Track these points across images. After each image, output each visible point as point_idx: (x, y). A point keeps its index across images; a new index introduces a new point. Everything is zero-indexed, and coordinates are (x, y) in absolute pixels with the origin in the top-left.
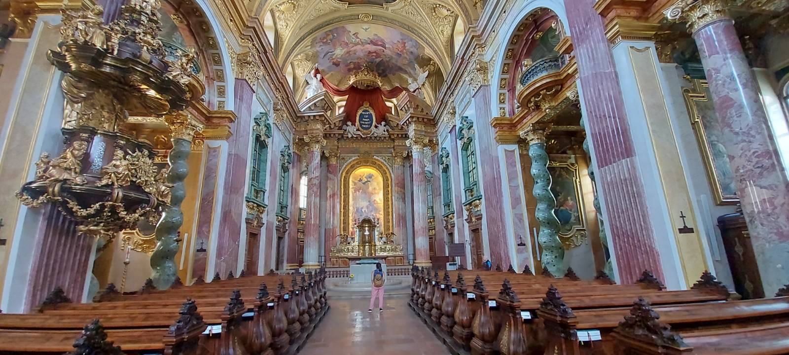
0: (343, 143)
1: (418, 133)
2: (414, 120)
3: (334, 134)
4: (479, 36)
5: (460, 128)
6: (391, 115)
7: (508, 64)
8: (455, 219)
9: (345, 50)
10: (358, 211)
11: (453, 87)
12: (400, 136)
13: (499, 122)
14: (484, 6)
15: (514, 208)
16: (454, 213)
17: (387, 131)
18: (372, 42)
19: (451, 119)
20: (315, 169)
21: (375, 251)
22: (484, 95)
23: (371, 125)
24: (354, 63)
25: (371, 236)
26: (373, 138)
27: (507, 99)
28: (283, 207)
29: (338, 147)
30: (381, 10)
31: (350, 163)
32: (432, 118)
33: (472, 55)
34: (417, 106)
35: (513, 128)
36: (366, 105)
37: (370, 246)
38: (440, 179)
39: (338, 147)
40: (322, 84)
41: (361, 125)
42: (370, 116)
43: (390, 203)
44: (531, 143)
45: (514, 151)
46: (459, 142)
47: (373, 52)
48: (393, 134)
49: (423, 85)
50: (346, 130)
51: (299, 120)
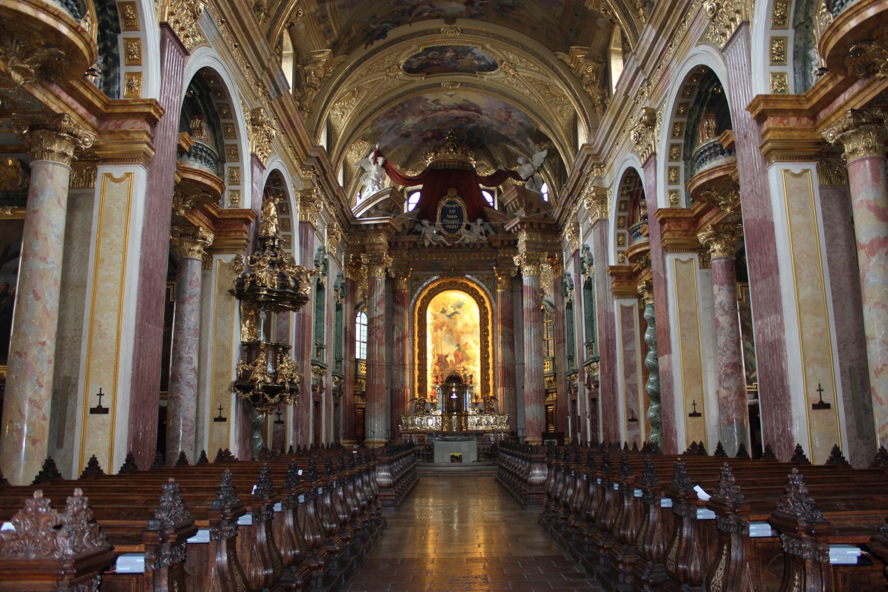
2: (525, 226)
3: (403, 243)
4: (596, 155)
6: (492, 210)
7: (626, 202)
8: (577, 381)
9: (420, 118)
10: (441, 360)
11: (575, 195)
12: (506, 243)
14: (604, 112)
17: (487, 233)
18: (460, 107)
20: (378, 304)
21: (466, 425)
23: (460, 226)
24: (433, 131)
25: (460, 401)
27: (627, 240)
28: (338, 361)
29: (409, 262)
30: (475, 78)
31: (428, 286)
33: (590, 172)
35: (633, 278)
36: (453, 192)
37: (459, 416)
40: (384, 171)
41: (444, 226)
42: (459, 211)
43: (490, 349)
45: (631, 308)
46: (582, 276)
47: (462, 118)
49: (542, 165)
51: (353, 229)
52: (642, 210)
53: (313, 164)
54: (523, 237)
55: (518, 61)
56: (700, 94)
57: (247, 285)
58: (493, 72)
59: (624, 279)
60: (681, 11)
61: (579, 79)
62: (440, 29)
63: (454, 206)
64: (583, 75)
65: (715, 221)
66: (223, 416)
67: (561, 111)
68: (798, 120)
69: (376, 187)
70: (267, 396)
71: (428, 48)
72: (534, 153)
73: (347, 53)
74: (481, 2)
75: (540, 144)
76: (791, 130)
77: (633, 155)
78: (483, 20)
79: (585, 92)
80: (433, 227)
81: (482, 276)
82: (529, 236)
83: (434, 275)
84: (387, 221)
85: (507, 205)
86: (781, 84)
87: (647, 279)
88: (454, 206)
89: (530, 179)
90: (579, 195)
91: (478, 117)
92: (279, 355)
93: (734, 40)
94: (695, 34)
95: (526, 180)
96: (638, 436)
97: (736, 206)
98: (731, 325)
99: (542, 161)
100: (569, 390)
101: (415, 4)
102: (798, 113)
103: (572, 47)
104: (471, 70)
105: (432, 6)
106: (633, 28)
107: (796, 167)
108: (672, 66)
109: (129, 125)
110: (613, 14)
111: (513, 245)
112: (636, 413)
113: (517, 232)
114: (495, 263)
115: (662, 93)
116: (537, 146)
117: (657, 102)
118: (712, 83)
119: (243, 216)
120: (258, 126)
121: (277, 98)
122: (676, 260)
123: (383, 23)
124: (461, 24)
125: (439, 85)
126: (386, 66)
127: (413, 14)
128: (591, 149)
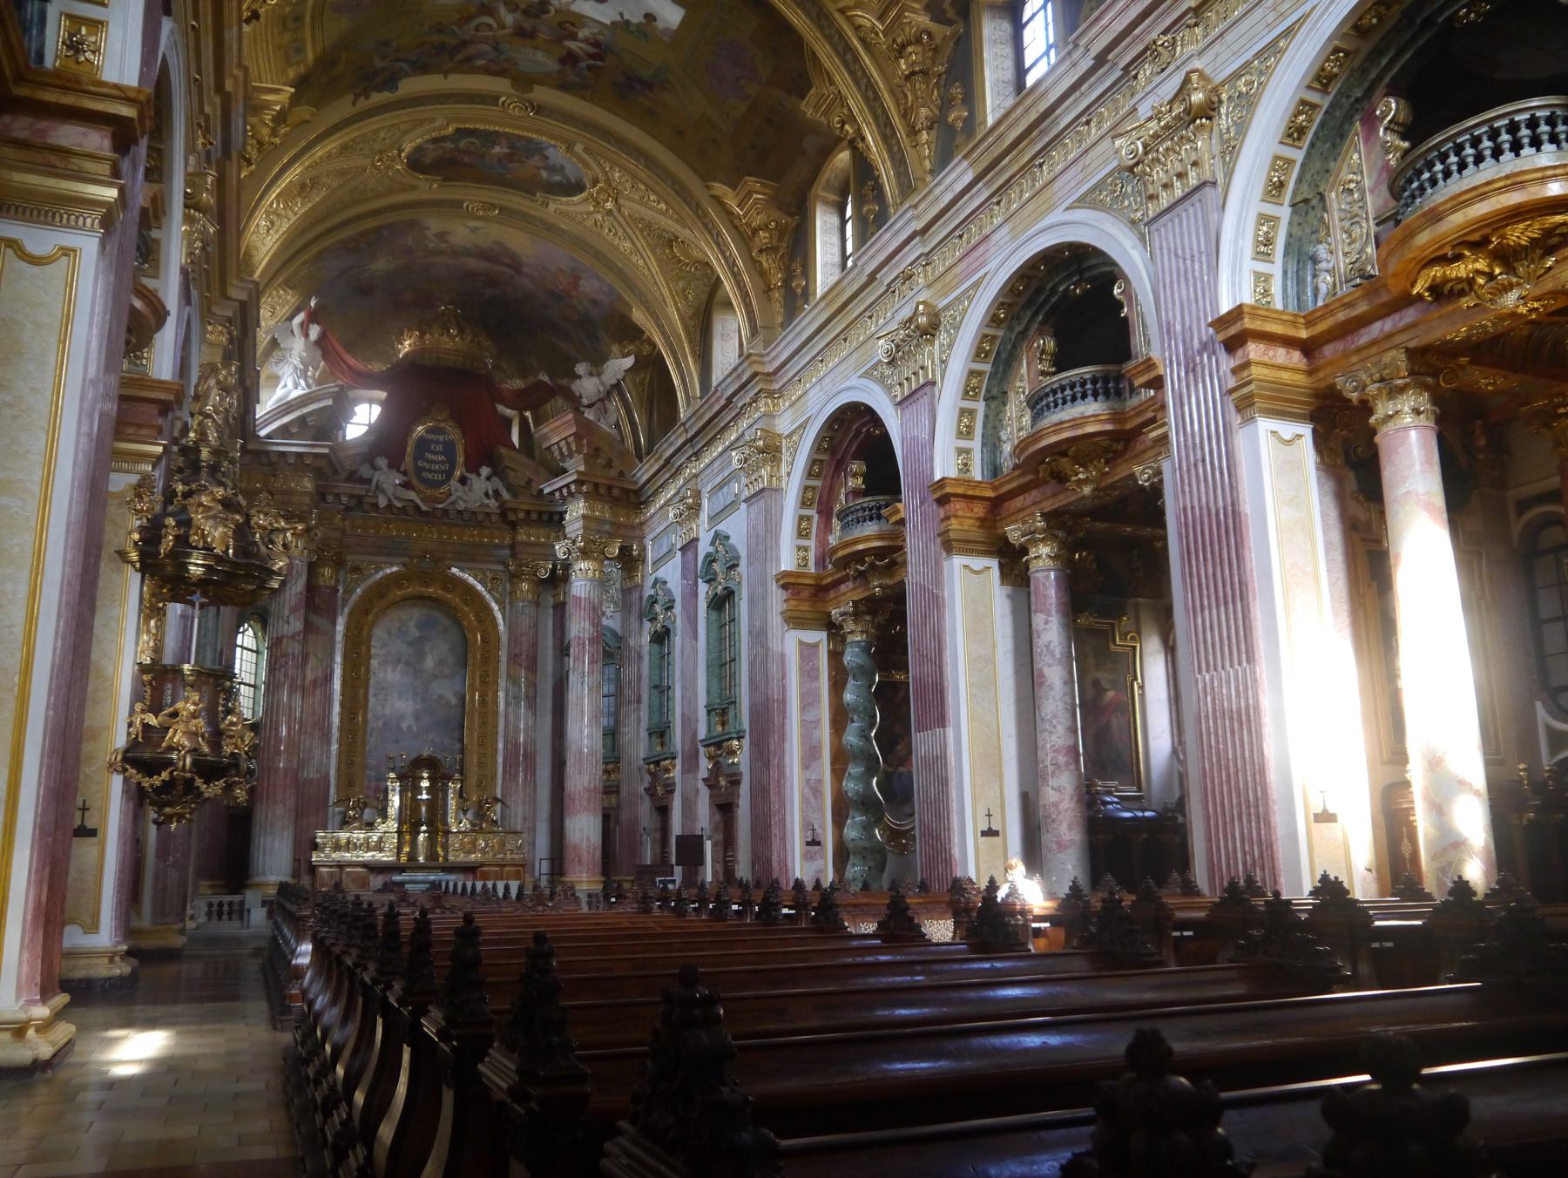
0: (360, 522)
1: (593, 525)
2: (585, 488)
3: (338, 496)
4: (769, 374)
5: (708, 555)
7: (821, 461)
12: (534, 516)
13: (792, 580)
15: (806, 765)
16: (674, 758)
18: (483, 254)
19: (689, 518)
21: (445, 847)
22: (767, 511)
23: (449, 474)
26: (452, 514)
32: (636, 488)
33: (750, 404)
34: (597, 450)
35: (821, 595)
37: (432, 834)
38: (640, 657)
39: (344, 531)
40: (319, 353)
41: (419, 470)
42: (449, 449)
44: (850, 638)
45: (816, 646)
46: (703, 588)
48: (515, 511)
50: (369, 481)
52: (850, 479)
53: (230, 314)
54: (576, 511)
55: (628, 185)
56: (1038, 291)
57: (169, 541)
58: (575, 199)
59: (805, 594)
60: (1039, 146)
61: (745, 238)
62: (498, 98)
63: (441, 438)
64: (755, 232)
65: (1048, 506)
66: (90, 825)
67: (684, 290)
68: (1288, 353)
69: (303, 383)
70: (199, 782)
71: (466, 129)
72: (605, 360)
73: (319, 103)
74: (592, 62)
75: (620, 343)
76: (1280, 367)
77: (865, 382)
78: (583, 98)
79: (754, 261)
80: (394, 472)
81: (483, 572)
82: (590, 508)
83: (392, 565)
84: (326, 451)
85: (549, 448)
86: (1266, 293)
87: (855, 598)
88: (441, 438)
89: (599, 405)
90: (708, 443)
91: (512, 278)
92: (222, 696)
93: (1178, 209)
94: (1067, 188)
95: (589, 406)
96: (823, 871)
97: (1103, 484)
98: (1065, 683)
99: (620, 376)
100: (651, 791)
101: (467, 37)
102: (1288, 342)
103: (747, 178)
104: (529, 187)
105: (497, 49)
106: (899, 162)
107: (1288, 429)
108: (996, 237)
109: (69, 135)
110: (859, 132)
111: (554, 521)
112: (819, 831)
113: (564, 499)
114: (507, 552)
115: (961, 282)
116: (615, 348)
117: (946, 295)
118: (1070, 276)
119: (162, 396)
120: (195, 210)
121: (218, 161)
122: (966, 567)
123: (397, 60)
124: (542, 94)
125: (459, 204)
126: (378, 146)
127: (459, 57)
128: (763, 363)
